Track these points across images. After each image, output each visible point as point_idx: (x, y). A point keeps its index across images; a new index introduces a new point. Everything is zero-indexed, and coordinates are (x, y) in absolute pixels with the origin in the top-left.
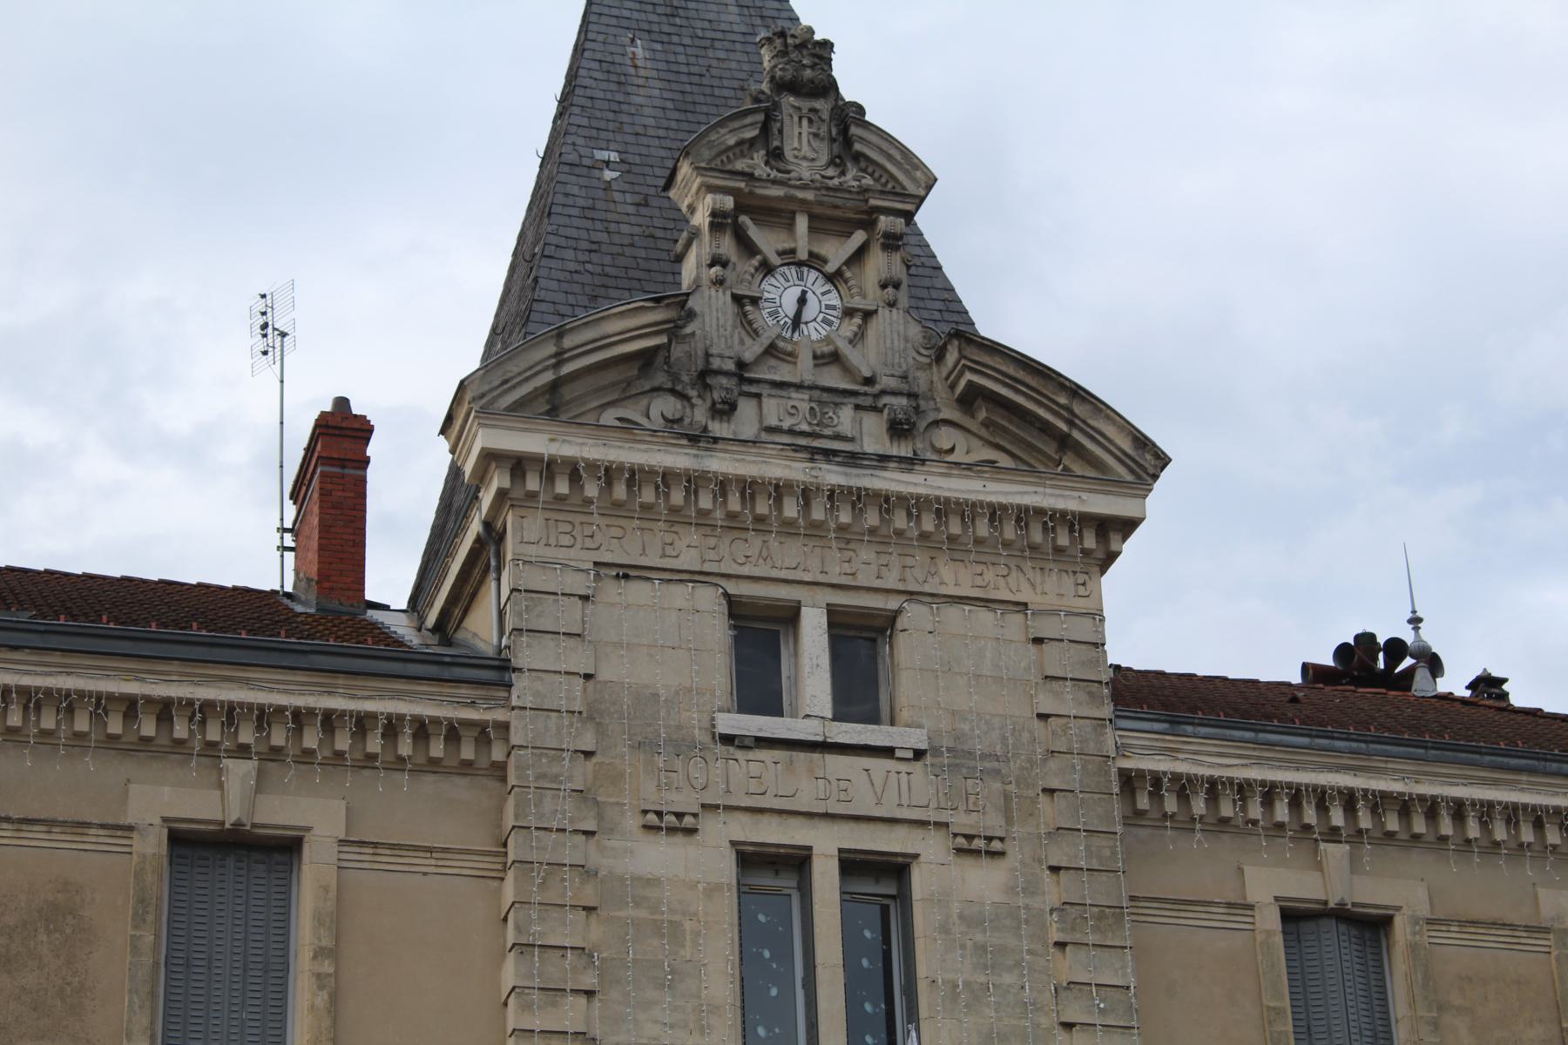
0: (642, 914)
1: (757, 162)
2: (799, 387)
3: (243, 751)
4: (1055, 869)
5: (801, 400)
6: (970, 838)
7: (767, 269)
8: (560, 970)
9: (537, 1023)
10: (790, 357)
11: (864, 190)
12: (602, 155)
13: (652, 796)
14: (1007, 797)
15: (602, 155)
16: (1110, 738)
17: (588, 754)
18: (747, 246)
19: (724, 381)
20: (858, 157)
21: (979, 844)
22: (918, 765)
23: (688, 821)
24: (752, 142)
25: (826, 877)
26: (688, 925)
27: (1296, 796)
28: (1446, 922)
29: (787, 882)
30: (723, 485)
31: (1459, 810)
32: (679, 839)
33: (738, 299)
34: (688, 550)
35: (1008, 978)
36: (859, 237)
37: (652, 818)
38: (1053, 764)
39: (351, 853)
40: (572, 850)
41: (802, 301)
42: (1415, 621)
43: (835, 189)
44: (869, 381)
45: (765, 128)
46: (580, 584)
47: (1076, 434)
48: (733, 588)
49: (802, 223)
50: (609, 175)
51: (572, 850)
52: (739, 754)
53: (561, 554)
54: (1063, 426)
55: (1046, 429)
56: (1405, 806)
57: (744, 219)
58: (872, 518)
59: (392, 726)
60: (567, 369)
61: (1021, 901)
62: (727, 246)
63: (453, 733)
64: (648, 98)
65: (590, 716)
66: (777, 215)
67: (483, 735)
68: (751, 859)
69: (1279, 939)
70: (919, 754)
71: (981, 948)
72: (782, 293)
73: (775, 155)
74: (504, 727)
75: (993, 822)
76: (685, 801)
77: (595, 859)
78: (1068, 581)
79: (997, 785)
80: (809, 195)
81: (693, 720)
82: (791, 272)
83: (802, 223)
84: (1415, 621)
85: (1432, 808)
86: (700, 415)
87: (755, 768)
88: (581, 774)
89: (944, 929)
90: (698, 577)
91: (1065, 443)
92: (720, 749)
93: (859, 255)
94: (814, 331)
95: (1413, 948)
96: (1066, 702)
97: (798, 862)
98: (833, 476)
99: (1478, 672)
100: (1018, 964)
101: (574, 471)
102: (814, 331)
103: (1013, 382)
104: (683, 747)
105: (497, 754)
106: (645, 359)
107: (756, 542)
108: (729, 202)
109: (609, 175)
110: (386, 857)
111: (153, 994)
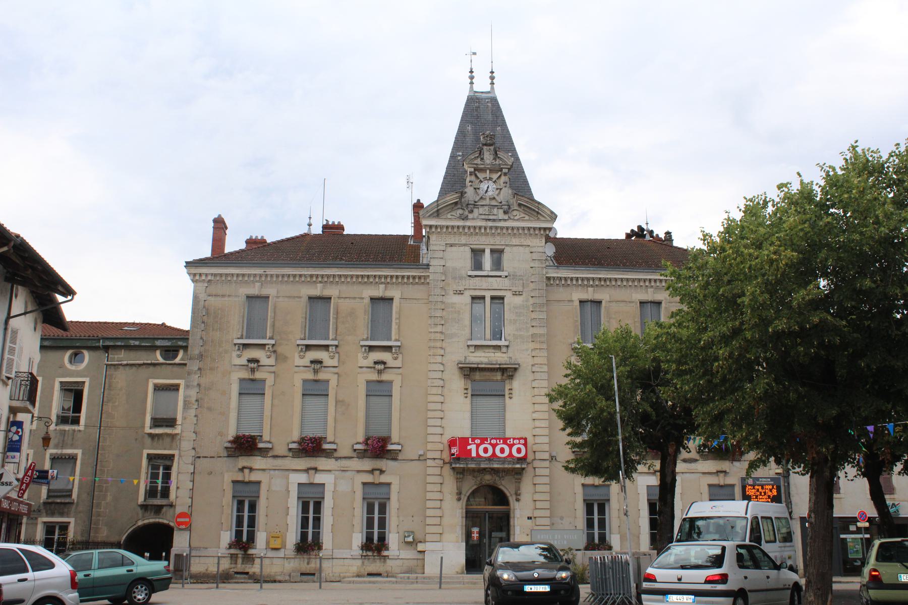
0: (453, 309)
1: (478, 161)
2: (486, 205)
3: (382, 283)
4: (532, 297)
5: (486, 208)
6: (515, 292)
7: (481, 182)
8: (438, 321)
9: (433, 330)
10: (485, 199)
11: (499, 165)
12: (458, 154)
13: (455, 288)
14: (523, 284)
15: (458, 154)
16: (544, 271)
17: (443, 280)
18: (477, 177)
19: (471, 206)
20: (499, 157)
21: (517, 293)
22: (506, 279)
23: (462, 292)
24: (478, 157)
25: (488, 300)
26: (461, 311)
27: (583, 279)
28: (612, 302)
29: (482, 301)
30: (469, 228)
31: (616, 280)
32: (460, 295)
33: (475, 189)
34: (463, 239)
35: (522, 318)
36: (500, 173)
37: (455, 292)
38: (533, 277)
39: (402, 300)
40: (440, 299)
41: (488, 187)
42: (647, 224)
43: (494, 165)
44: (501, 203)
45: (480, 154)
46: (443, 248)
47: (540, 211)
48: (472, 247)
49: (488, 171)
50: (459, 158)
51: (440, 299)
52: (472, 279)
53: (438, 243)
54: (537, 210)
55: (534, 210)
56: (605, 280)
57: (476, 172)
58: (499, 231)
59: (408, 277)
60: (439, 208)
61: (525, 303)
62: (473, 178)
63: (420, 277)
64: (470, 139)
65: (444, 273)
66: (483, 170)
67: (426, 277)
68: (474, 298)
69: (578, 307)
70: (506, 277)
71: (517, 313)
72: (484, 186)
73: (482, 159)
74: (429, 276)
75: (520, 289)
76: (461, 288)
77: (444, 300)
78: (538, 240)
79: (521, 282)
80: (489, 166)
81: (463, 273)
82: (486, 182)
83: (488, 171)
84: (647, 224)
85: (610, 280)
86: (466, 213)
87: (475, 281)
88: (442, 284)
89: (510, 309)
90: (465, 245)
91: (538, 213)
92: (468, 278)
93: (500, 176)
94: (490, 193)
95: (605, 307)
96: (536, 264)
97: (483, 298)
98: (490, 224)
99: (666, 231)
100: (524, 315)
101: (442, 227)
102: (490, 193)
103: (527, 202)
104: (461, 278)
105: (428, 281)
106: (456, 203)
107: (477, 237)
108: (472, 170)
109: (459, 158)
110: (408, 301)
111: (368, 327)
